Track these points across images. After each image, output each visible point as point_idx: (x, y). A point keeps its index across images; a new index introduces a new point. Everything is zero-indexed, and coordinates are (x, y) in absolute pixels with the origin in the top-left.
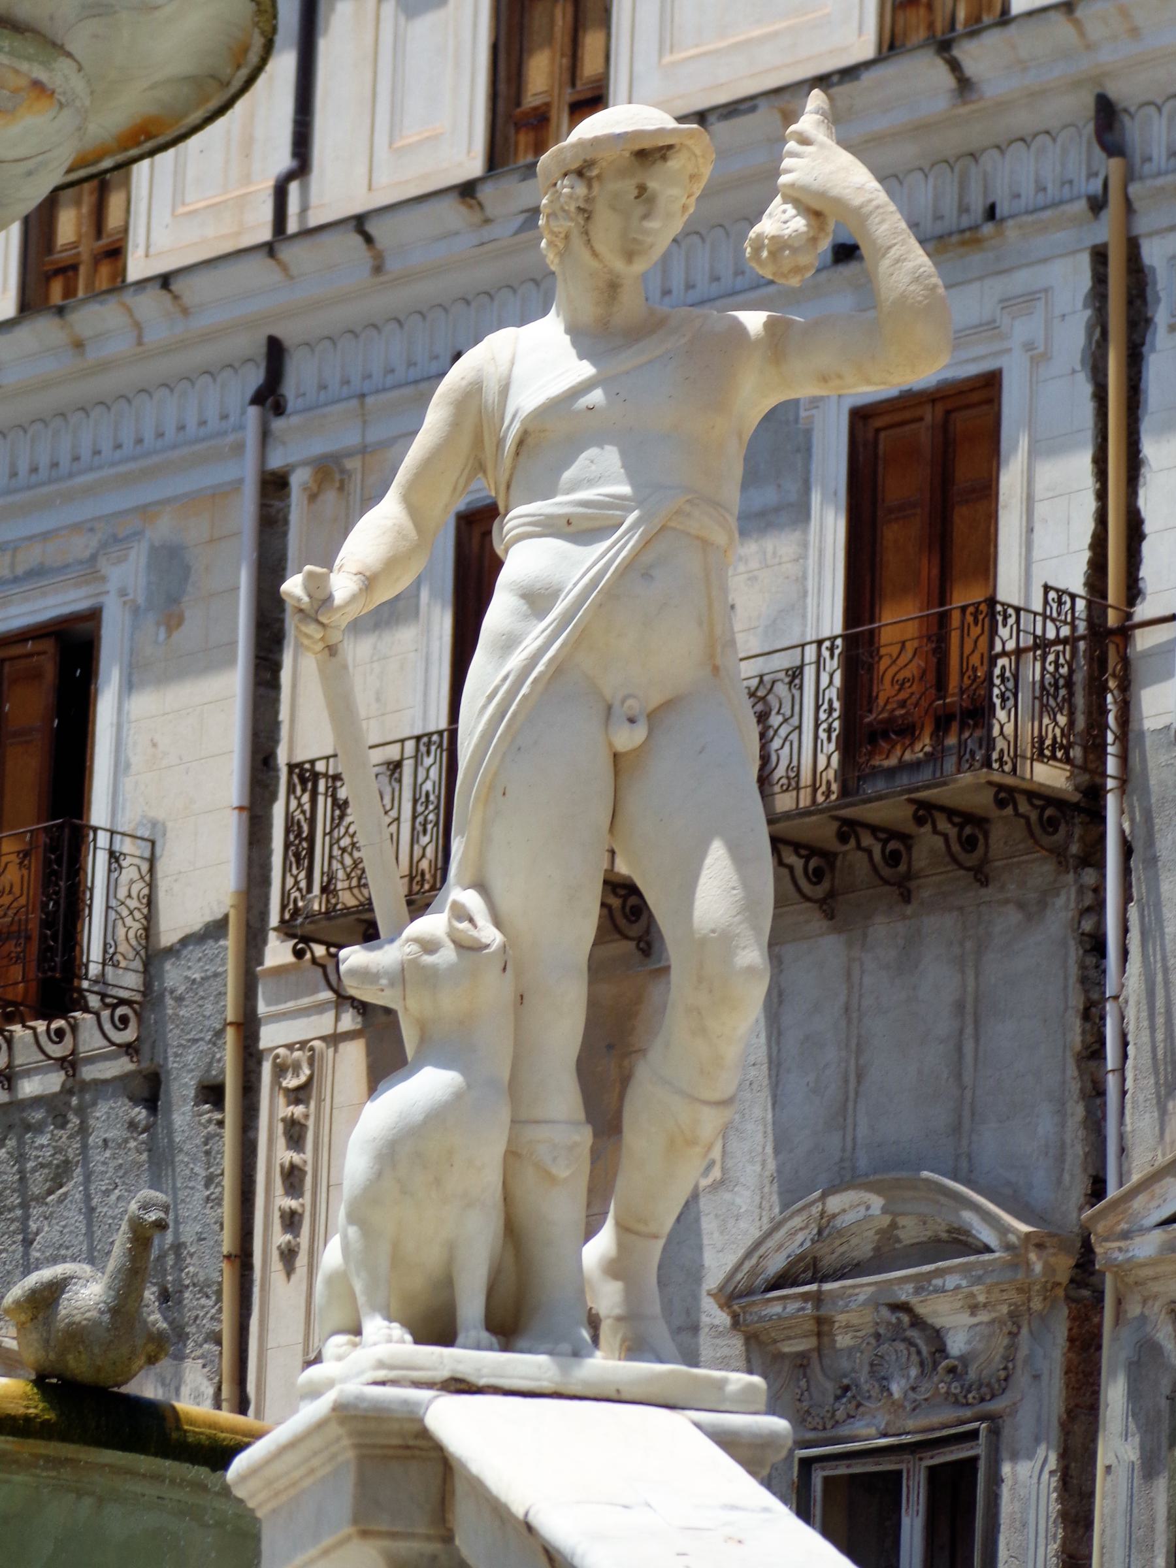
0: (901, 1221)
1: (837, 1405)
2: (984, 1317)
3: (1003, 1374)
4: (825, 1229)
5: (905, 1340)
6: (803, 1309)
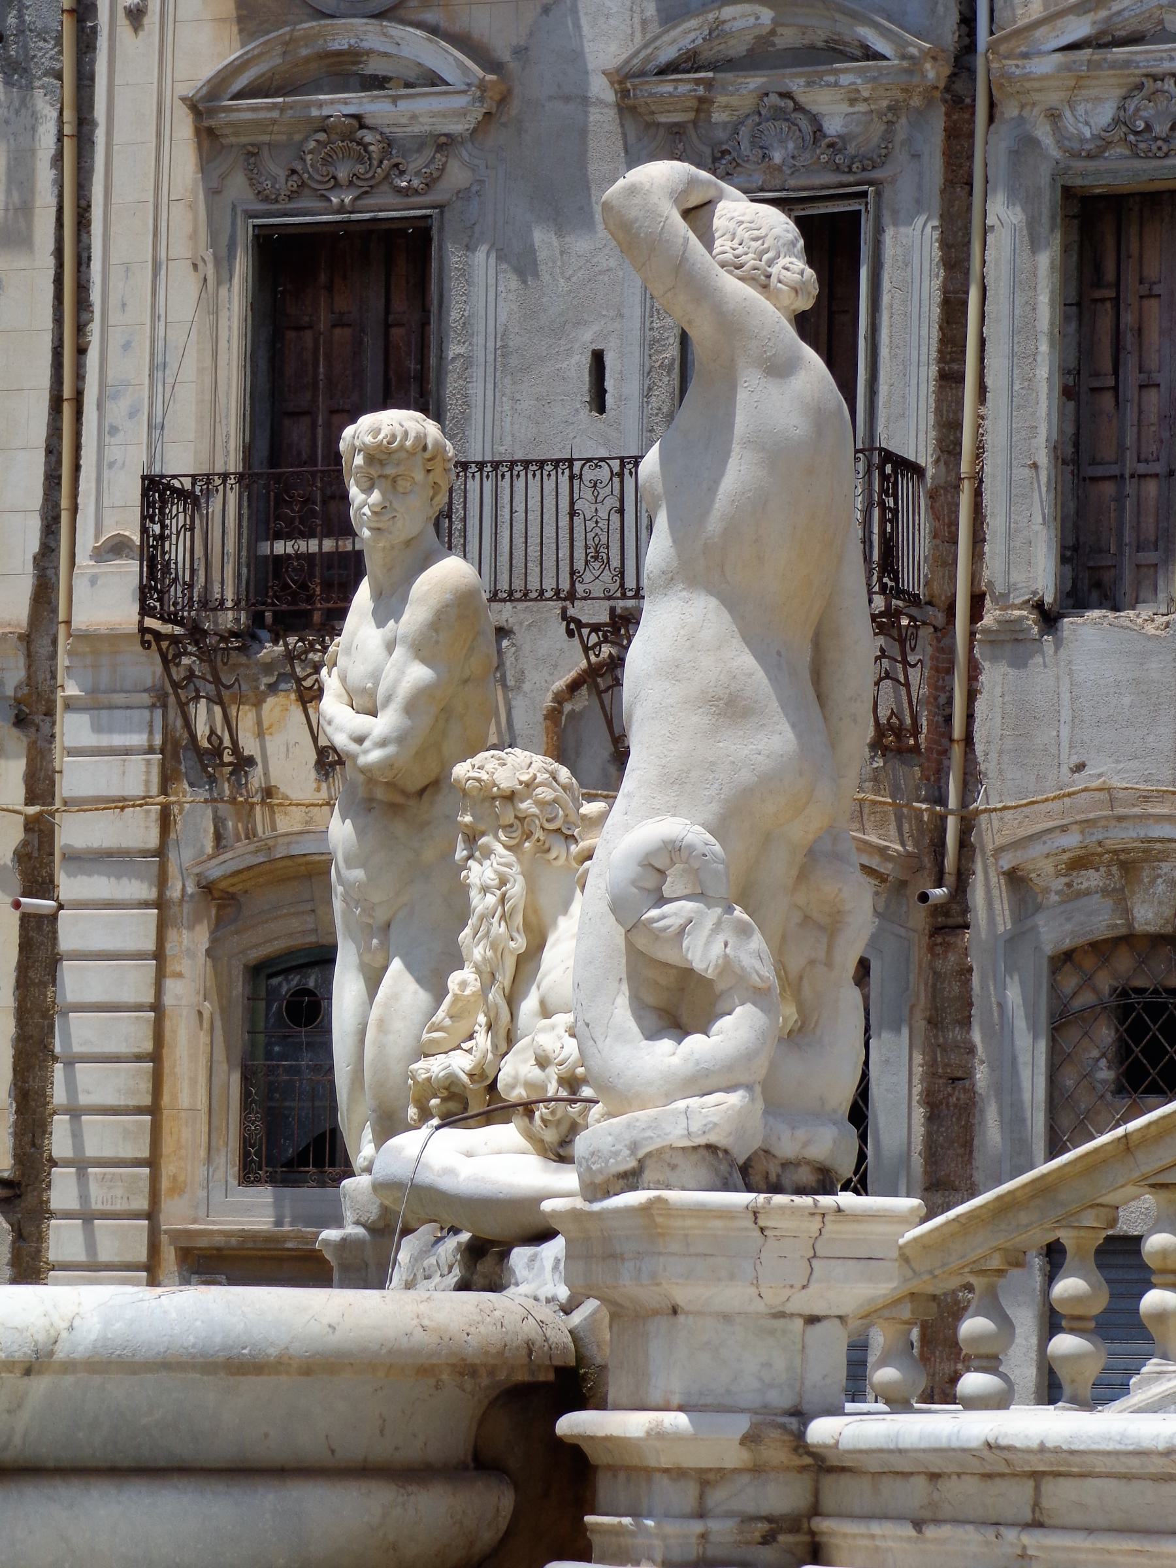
0: (780, 30)
1: (717, 165)
2: (862, 107)
3: (884, 152)
4: (716, 31)
5: (787, 120)
6: (695, 90)
